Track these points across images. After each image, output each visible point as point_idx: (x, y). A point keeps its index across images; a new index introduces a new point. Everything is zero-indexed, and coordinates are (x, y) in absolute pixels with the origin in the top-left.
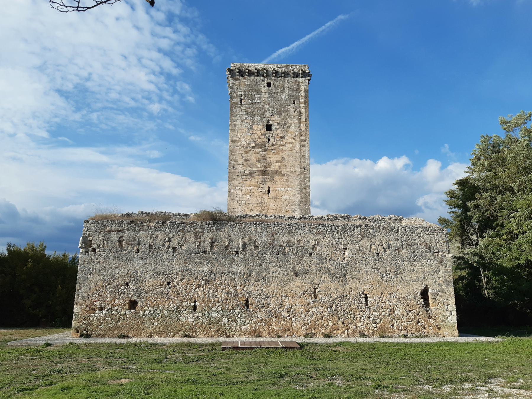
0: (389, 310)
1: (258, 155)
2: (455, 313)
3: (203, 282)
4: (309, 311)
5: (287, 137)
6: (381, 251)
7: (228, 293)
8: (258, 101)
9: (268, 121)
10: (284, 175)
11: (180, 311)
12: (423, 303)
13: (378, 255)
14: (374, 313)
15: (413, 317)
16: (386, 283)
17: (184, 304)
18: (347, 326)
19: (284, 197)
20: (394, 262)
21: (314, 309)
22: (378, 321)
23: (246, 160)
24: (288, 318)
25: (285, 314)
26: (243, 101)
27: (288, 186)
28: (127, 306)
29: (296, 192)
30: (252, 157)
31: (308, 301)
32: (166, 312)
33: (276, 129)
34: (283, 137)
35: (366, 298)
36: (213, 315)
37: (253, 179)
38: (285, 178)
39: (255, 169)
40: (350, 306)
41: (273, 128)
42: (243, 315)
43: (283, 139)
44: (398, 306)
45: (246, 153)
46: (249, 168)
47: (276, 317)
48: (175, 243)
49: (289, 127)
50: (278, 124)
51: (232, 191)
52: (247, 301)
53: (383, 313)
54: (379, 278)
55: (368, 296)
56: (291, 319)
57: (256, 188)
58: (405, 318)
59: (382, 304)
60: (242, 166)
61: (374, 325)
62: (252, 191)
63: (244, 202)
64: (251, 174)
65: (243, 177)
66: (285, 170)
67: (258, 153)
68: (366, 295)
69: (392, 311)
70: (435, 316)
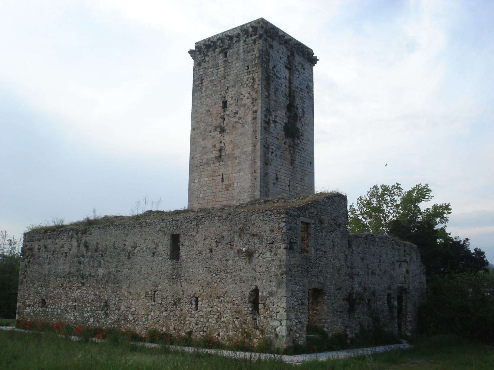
0: (216, 317)
1: (214, 140)
2: (284, 323)
3: (80, 285)
4: (148, 315)
5: (240, 112)
6: (214, 245)
7: (95, 295)
8: (216, 78)
9: (225, 97)
10: (236, 158)
11: (67, 310)
12: (251, 309)
13: (211, 251)
14: (202, 320)
15: (239, 326)
16: (216, 284)
17: (69, 304)
18: (178, 332)
19: (236, 185)
20: (224, 259)
21: (152, 313)
22: (205, 330)
23: (203, 148)
24: (133, 321)
25: (131, 318)
26: (203, 81)
27: (240, 171)
28: (41, 304)
29: (247, 177)
30: (208, 144)
31: (148, 304)
32: (59, 311)
33: (231, 104)
34: (236, 113)
35: (197, 301)
36: (86, 315)
37: (209, 169)
38: (237, 161)
39: (212, 156)
40: (182, 310)
41: (228, 104)
42: (103, 317)
43: (237, 115)
44: (225, 312)
45: (204, 139)
46: (206, 157)
47: (124, 320)
48: (66, 249)
49: (242, 99)
50: (232, 97)
51: (192, 184)
52: (106, 303)
53: (210, 320)
54: (209, 278)
55: (199, 299)
56: (135, 322)
57: (211, 178)
58: (231, 326)
59: (210, 309)
60: (199, 155)
61: (201, 333)
62: (208, 182)
63: (201, 196)
64: (207, 163)
65: (201, 167)
66: (237, 152)
67: (214, 137)
68: (197, 298)
69: (219, 317)
70: (262, 326)
